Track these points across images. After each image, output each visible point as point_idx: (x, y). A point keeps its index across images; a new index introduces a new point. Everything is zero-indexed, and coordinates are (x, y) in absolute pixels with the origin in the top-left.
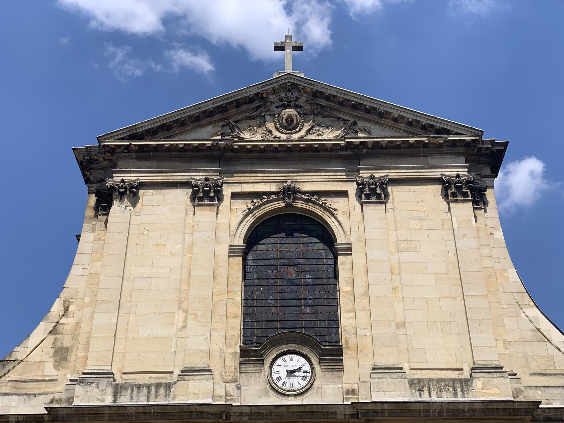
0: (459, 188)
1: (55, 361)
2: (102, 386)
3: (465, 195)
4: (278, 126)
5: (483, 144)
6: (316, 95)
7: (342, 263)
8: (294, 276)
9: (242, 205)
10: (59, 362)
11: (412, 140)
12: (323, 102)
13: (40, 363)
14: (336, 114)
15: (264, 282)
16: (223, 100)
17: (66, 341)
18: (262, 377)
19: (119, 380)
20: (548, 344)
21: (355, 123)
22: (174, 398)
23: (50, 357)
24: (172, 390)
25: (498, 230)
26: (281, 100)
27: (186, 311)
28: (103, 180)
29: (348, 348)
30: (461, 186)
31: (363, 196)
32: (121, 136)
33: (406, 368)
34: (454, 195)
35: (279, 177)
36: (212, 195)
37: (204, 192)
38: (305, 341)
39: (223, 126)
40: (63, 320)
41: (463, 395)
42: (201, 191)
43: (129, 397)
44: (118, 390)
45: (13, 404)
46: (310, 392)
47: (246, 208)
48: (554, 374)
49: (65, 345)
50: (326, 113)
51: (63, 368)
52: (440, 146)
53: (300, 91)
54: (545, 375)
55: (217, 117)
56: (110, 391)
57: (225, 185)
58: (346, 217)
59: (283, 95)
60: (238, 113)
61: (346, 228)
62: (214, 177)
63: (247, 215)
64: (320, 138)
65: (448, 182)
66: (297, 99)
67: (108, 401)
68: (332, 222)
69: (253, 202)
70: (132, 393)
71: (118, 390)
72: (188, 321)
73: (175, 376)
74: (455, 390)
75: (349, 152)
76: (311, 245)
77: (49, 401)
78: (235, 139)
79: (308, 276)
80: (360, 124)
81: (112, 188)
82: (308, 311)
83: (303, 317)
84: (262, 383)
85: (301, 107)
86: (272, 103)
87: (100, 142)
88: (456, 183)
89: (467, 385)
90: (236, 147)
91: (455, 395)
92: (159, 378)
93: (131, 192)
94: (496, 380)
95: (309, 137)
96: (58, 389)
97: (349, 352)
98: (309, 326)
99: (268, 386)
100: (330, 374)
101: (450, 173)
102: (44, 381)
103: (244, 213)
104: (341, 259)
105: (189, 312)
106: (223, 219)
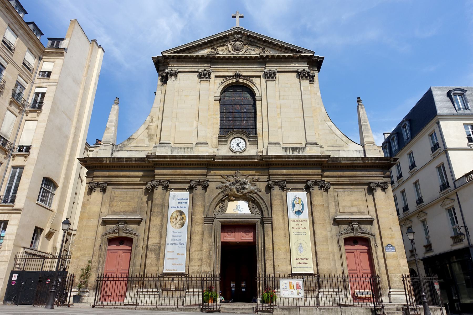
0: (304, 75)
1: (149, 139)
2: (167, 148)
3: (306, 77)
4: (233, 49)
5: (314, 58)
6: (249, 36)
7: (258, 104)
8: (239, 109)
9: (219, 80)
10: (150, 139)
11: (287, 55)
12: (252, 40)
13: (143, 139)
14: (256, 44)
15: (228, 111)
16: (211, 38)
17: (153, 132)
18: (227, 146)
19: (173, 146)
20: (335, 135)
24: (193, 150)
25: (319, 92)
26: (235, 38)
28: (164, 70)
29: (260, 136)
30: (305, 74)
33: (281, 143)
34: (302, 77)
35: (234, 70)
36: (207, 76)
37: (204, 75)
38: (243, 133)
39: (211, 49)
40: (151, 124)
41: (302, 152)
42: (203, 75)
43: (177, 152)
45: (134, 154)
46: (245, 152)
48: (336, 146)
49: (152, 133)
50: (252, 44)
51: (152, 141)
52: (298, 58)
53: (242, 35)
54: (333, 146)
55: (209, 45)
56: (170, 150)
57: (212, 72)
59: (235, 36)
60: (218, 44)
61: (260, 91)
62: (208, 69)
63: (221, 84)
64: (250, 54)
65: (300, 73)
66: (241, 38)
67: (169, 153)
68: (254, 88)
71: (173, 149)
73: (194, 145)
75: (261, 60)
76: (246, 97)
78: (216, 54)
79: (245, 109)
81: (167, 73)
82: (245, 122)
84: (227, 148)
86: (231, 40)
87: (162, 54)
89: (303, 149)
90: (217, 57)
91: (299, 153)
93: (175, 75)
94: (314, 147)
95: (246, 54)
96: (150, 149)
97: (260, 138)
98: (245, 128)
99: (229, 150)
100: (253, 146)
101: (301, 69)
103: (220, 84)
104: (257, 102)
106: (212, 86)
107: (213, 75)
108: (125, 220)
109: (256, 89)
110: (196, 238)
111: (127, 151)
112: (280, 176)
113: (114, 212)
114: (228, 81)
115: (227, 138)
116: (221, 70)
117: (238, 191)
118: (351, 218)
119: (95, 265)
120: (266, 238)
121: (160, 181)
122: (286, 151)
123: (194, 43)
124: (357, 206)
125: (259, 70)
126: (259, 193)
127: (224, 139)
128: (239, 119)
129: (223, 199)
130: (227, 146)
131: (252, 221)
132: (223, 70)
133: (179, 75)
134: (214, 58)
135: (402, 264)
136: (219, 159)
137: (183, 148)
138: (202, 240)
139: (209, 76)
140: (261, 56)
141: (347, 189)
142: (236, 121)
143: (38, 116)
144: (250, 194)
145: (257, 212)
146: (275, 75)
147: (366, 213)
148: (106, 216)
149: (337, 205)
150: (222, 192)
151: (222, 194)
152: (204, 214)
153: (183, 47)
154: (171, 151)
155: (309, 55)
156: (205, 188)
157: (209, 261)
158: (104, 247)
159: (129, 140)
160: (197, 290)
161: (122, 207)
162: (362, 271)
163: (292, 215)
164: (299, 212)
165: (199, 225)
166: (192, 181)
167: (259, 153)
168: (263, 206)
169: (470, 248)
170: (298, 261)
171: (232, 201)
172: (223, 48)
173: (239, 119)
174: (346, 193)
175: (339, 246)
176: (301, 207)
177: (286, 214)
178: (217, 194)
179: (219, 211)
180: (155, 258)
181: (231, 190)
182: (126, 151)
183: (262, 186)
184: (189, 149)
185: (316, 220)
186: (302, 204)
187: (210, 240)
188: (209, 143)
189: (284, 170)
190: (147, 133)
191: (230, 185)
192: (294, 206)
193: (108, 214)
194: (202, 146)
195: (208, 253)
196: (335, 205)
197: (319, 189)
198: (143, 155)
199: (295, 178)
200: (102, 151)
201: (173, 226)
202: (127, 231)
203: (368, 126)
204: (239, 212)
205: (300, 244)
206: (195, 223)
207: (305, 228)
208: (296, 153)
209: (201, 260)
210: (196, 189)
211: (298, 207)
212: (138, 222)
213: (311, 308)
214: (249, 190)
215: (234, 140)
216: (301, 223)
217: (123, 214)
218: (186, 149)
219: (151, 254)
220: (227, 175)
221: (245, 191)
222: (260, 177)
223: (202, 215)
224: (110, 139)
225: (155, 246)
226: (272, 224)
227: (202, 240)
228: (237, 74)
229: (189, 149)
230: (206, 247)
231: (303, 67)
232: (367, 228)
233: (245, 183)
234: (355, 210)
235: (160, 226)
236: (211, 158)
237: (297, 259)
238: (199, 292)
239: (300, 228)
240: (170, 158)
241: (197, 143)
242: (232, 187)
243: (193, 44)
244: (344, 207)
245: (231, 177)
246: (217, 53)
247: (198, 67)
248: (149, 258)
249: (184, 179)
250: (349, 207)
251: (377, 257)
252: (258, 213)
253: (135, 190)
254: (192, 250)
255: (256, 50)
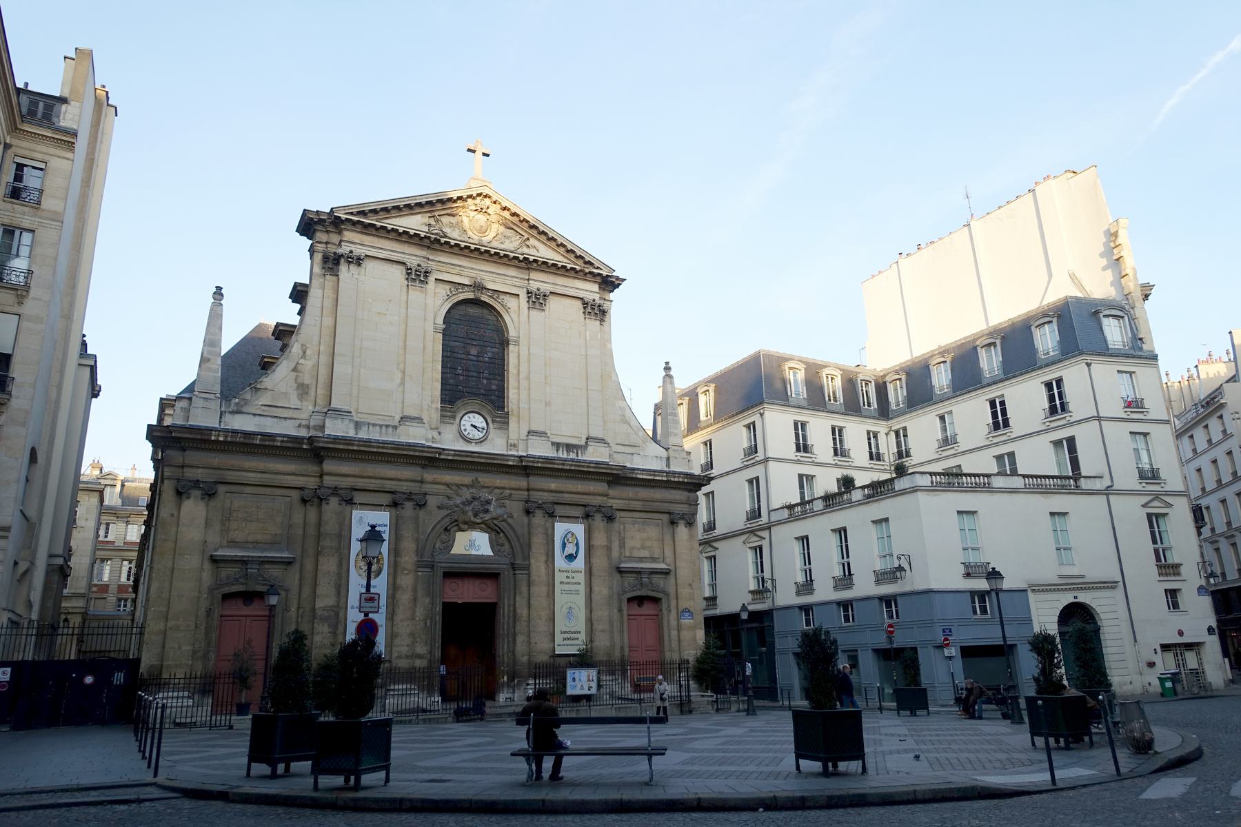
1: (298, 394)
2: (346, 422)
7: (512, 352)
9: (443, 290)
11: (569, 266)
13: (286, 393)
17: (307, 379)
19: (356, 419)
21: (528, 239)
22: (399, 438)
23: (294, 390)
27: (404, 372)
31: (531, 303)
32: (351, 211)
40: (302, 361)
43: (366, 432)
44: (358, 425)
46: (486, 442)
47: (445, 294)
48: (629, 445)
49: (305, 382)
51: (306, 400)
55: (427, 209)
56: (352, 426)
58: (516, 315)
61: (516, 324)
67: (351, 433)
69: (450, 289)
70: (368, 430)
71: (358, 425)
72: (406, 380)
74: (577, 453)
75: (523, 264)
77: (297, 425)
80: (532, 242)
83: (480, 386)
85: (489, 214)
88: (592, 305)
91: (577, 456)
92: (384, 420)
99: (458, 435)
100: (499, 431)
101: (589, 297)
102: (290, 408)
105: (406, 374)
107: (432, 279)
108: (261, 559)
109: (510, 320)
110: (404, 598)
111: (254, 415)
112: (545, 494)
113: (233, 543)
114: (460, 295)
115: (454, 412)
116: (448, 270)
117: (476, 515)
118: (642, 568)
119: (200, 647)
120: (517, 598)
121: (336, 488)
122: (557, 451)
123: (400, 202)
124: (649, 547)
125: (518, 284)
126: (509, 520)
127: (450, 412)
128: (475, 374)
129: (449, 528)
130: (455, 427)
131: (496, 569)
132: (451, 270)
133: (364, 264)
134: (437, 241)
135: (698, 637)
136: (448, 455)
137: (379, 425)
138: (415, 600)
139: (426, 277)
140: (525, 257)
141: (638, 520)
142: (470, 379)
143: (20, 303)
144: (495, 522)
145: (504, 553)
146: (545, 300)
147: (660, 560)
148: (216, 550)
149: (622, 546)
150: (449, 514)
151: (447, 520)
152: (417, 555)
153: (377, 205)
154: (356, 429)
155: (605, 274)
156: (421, 505)
157: (423, 637)
158: (216, 611)
159: (256, 391)
160: (409, 686)
161: (249, 533)
162: (646, 647)
163: (560, 562)
164: (571, 558)
165: (407, 574)
166: (397, 492)
167: (511, 446)
168: (515, 544)
169: (774, 612)
170: (566, 636)
171: (463, 531)
172: (452, 221)
173: (475, 374)
174: (637, 526)
175: (620, 610)
176: (575, 548)
177: (550, 559)
178: (439, 518)
179: (441, 550)
180: (330, 633)
181: (464, 512)
182: (251, 416)
183: (516, 508)
184: (390, 430)
185: (594, 570)
186: (577, 544)
187: (427, 600)
188: (424, 421)
189: (553, 483)
190: (294, 381)
191: (463, 503)
192: (564, 546)
193: (221, 546)
194: (414, 424)
195: (422, 624)
196: (620, 546)
197: (603, 520)
198: (287, 429)
199: (568, 499)
200: (200, 409)
201: (360, 575)
202: (264, 580)
203: (676, 416)
204: (474, 552)
205: (570, 608)
206: (402, 571)
207: (578, 584)
208: (572, 456)
209: (412, 635)
210: (403, 508)
211: (570, 549)
212: (289, 563)
213: (602, 707)
214: (494, 515)
215: (466, 416)
216: (573, 574)
217: (253, 548)
218: (384, 428)
219: (321, 625)
220: (458, 486)
221: (487, 517)
222: (513, 492)
223: (413, 555)
224: (213, 386)
225: (328, 611)
226: (529, 574)
227: (415, 600)
228: (477, 284)
229: (390, 430)
230: (420, 613)
231: (590, 290)
232: (658, 581)
233: (488, 502)
234: (645, 553)
235: (336, 574)
236: (436, 453)
237: (564, 633)
238: (411, 689)
239: (571, 583)
240: (358, 445)
241: (404, 418)
242: (467, 508)
243: (397, 202)
244: (632, 548)
245: (465, 489)
246: (441, 231)
247: (403, 253)
248: (318, 633)
249: (381, 486)
250: (639, 549)
251: (668, 627)
252: (505, 555)
253: (274, 499)
254: (398, 617)
255: (513, 240)
